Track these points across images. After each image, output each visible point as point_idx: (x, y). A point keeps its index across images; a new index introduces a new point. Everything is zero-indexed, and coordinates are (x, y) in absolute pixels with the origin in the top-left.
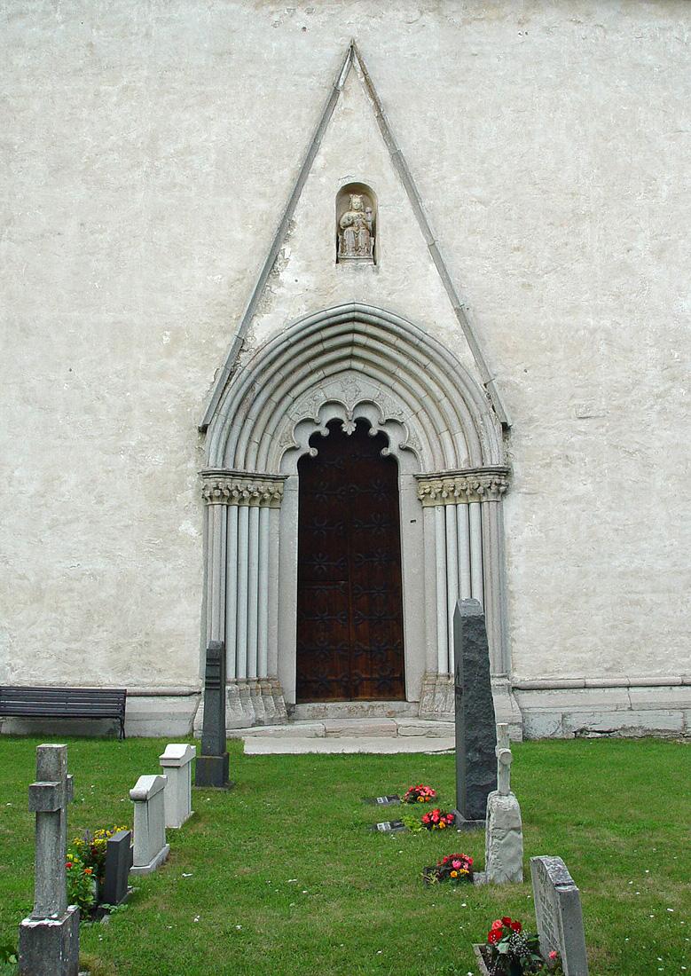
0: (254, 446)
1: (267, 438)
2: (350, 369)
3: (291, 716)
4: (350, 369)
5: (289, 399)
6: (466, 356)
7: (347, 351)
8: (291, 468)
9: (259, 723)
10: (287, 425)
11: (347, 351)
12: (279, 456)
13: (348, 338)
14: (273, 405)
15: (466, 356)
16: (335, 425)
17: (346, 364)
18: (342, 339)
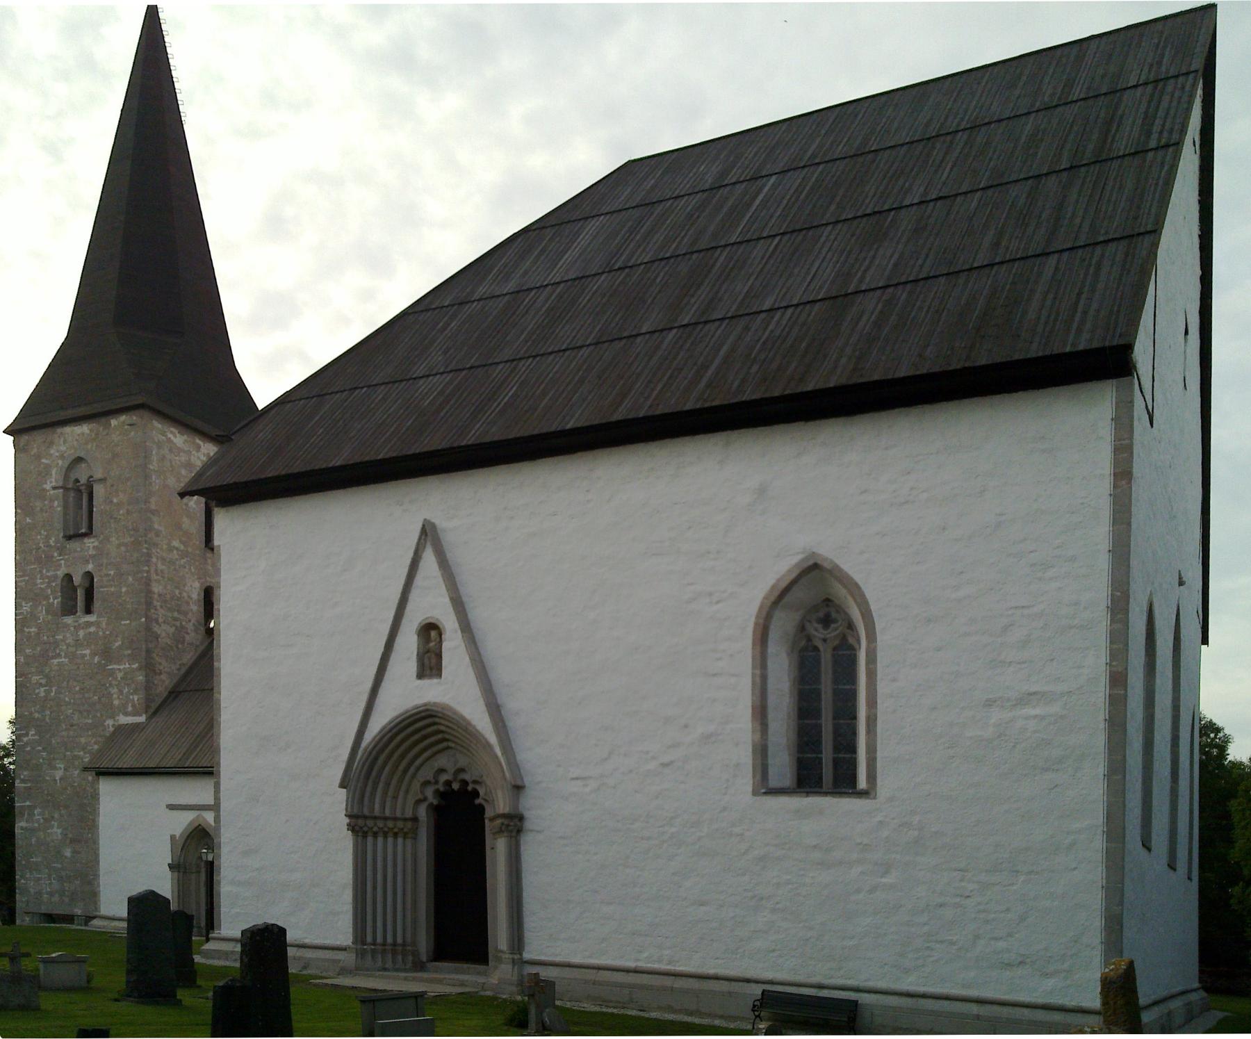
0: (389, 800)
1: (401, 794)
2: (448, 748)
3: (419, 966)
4: (448, 748)
5: (412, 769)
6: (492, 739)
7: (440, 736)
8: (422, 811)
9: (385, 969)
10: (416, 785)
11: (440, 736)
12: (414, 801)
13: (435, 728)
14: (399, 773)
15: (492, 739)
16: (448, 783)
17: (445, 744)
18: (426, 730)
